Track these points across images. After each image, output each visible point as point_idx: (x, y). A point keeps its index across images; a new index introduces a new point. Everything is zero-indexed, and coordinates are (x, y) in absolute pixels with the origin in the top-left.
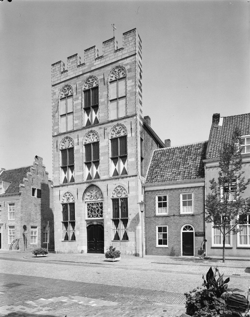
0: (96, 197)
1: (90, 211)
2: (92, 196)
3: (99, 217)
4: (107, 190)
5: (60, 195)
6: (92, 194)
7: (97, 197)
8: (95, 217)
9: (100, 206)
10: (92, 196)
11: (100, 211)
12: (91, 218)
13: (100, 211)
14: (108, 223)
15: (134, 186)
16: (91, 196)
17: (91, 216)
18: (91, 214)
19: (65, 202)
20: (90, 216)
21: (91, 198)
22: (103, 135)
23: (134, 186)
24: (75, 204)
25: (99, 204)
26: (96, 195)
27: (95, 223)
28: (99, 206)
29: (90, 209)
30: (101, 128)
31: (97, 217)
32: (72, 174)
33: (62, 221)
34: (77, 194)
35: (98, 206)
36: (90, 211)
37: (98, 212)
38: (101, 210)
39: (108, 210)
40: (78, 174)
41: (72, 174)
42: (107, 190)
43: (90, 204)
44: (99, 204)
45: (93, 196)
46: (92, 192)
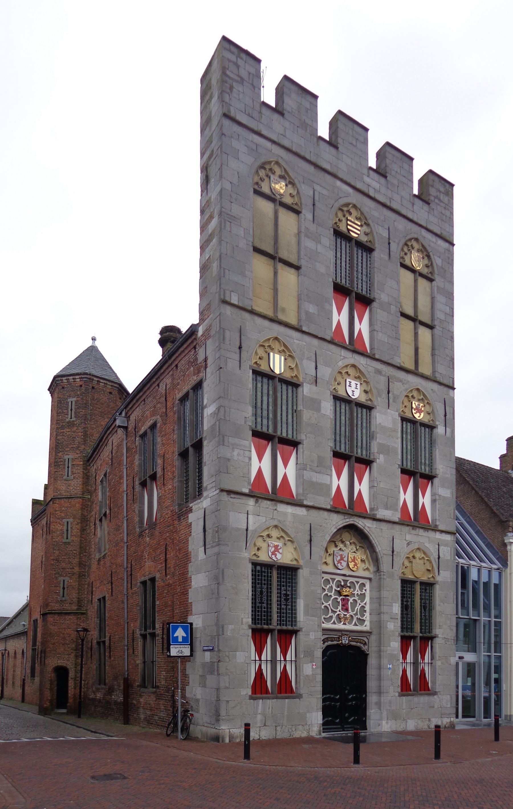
0: (353, 563)
1: (330, 602)
2: (342, 559)
3: (355, 625)
4: (393, 552)
5: (247, 530)
6: (341, 553)
7: (356, 565)
8: (344, 624)
9: (359, 593)
10: (342, 559)
11: (358, 607)
12: (334, 623)
13: (358, 607)
14: (391, 643)
15: (449, 558)
16: (339, 558)
17: (334, 619)
18: (333, 611)
19: (264, 557)
20: (331, 617)
21: (339, 562)
22: (385, 395)
23: (449, 558)
24: (303, 575)
25: (357, 587)
26: (354, 557)
27: (345, 641)
28: (356, 592)
29: (331, 596)
30: (379, 372)
31: (350, 623)
32: (284, 471)
33: (249, 620)
34: (311, 541)
35: (354, 590)
36: (330, 602)
37: (353, 610)
38: (362, 604)
39: (394, 609)
40: (314, 480)
41: (284, 471)
42: (393, 552)
43: (333, 580)
44: (357, 587)
45: (346, 559)
46: (341, 546)
